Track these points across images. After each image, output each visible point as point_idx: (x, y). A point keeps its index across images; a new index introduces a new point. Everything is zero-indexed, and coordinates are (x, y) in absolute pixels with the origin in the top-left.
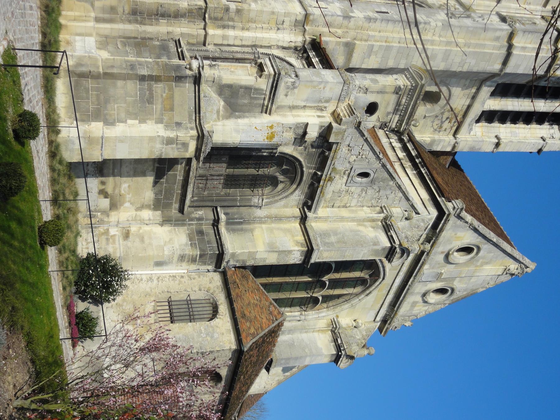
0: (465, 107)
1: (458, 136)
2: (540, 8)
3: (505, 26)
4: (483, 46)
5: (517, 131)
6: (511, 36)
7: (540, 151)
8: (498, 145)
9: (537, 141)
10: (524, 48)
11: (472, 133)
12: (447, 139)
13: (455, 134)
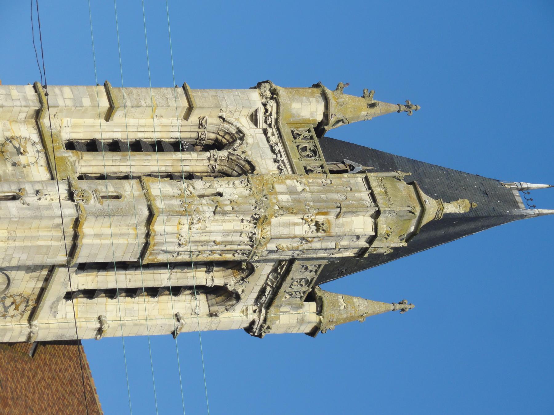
0: (37, 291)
1: (35, 322)
2: (177, 121)
3: (70, 210)
4: (38, 238)
5: (136, 307)
6: (77, 223)
7: (173, 333)
8: (100, 331)
9: (167, 322)
10: (98, 236)
11: (59, 316)
12: (17, 328)
13: (31, 318)
